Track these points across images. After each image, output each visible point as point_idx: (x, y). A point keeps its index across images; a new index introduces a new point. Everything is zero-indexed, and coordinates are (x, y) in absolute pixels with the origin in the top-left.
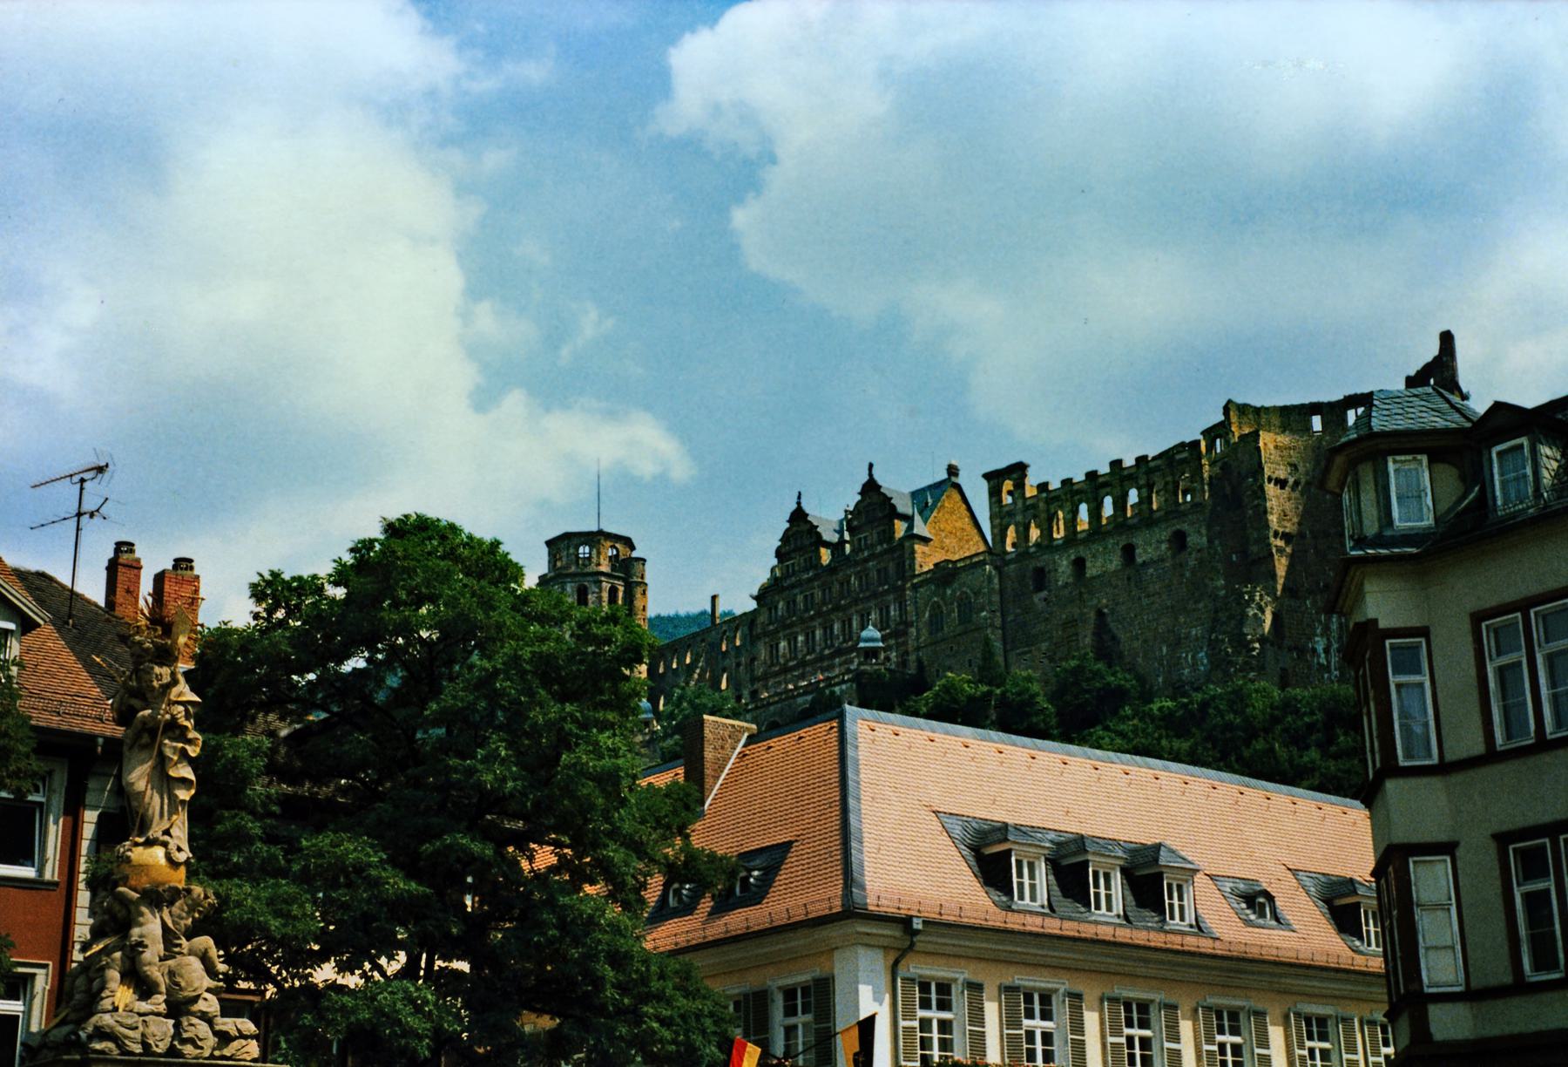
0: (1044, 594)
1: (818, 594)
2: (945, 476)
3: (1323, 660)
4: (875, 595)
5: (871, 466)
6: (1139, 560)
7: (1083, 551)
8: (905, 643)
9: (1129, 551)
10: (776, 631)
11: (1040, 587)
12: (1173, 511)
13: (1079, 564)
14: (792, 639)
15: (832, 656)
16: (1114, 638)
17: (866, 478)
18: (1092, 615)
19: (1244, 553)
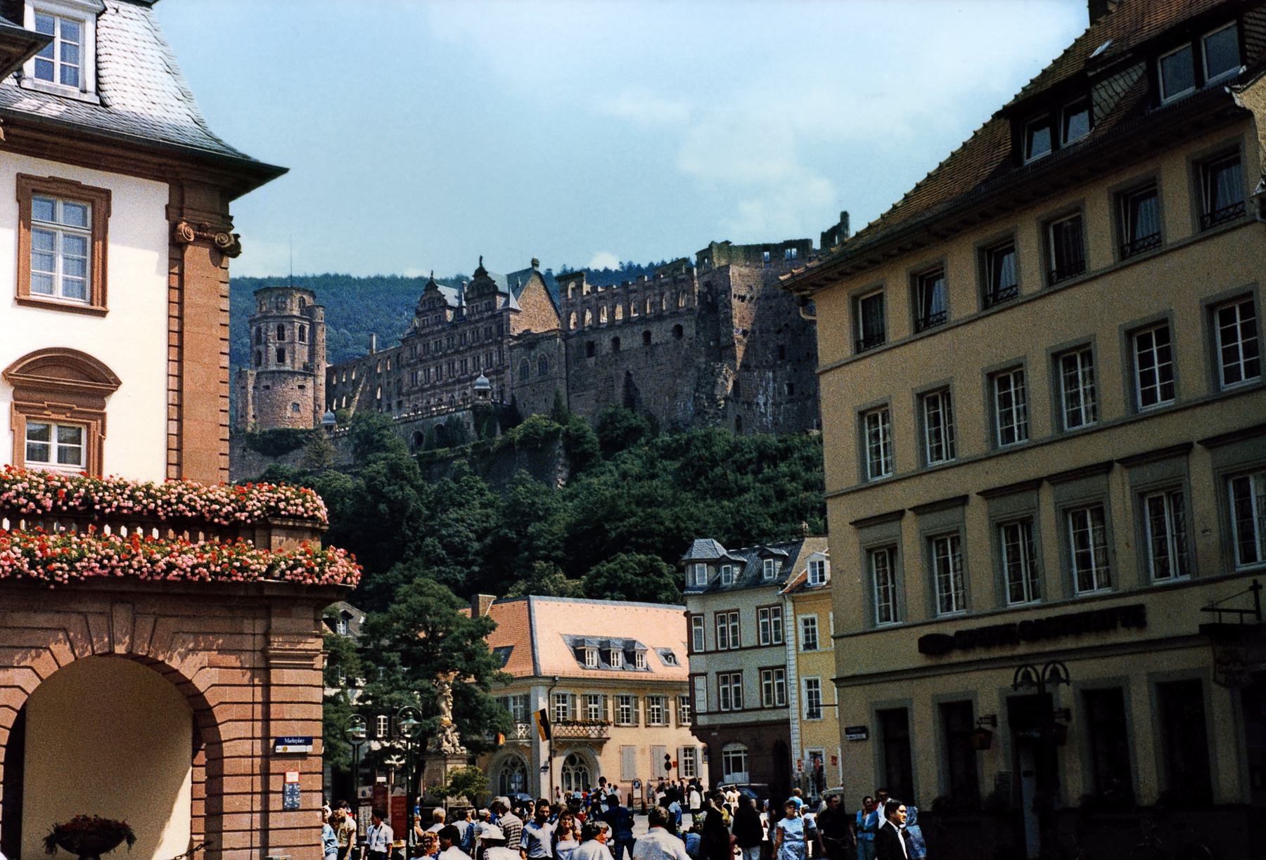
0: (592, 360)
1: (445, 342)
2: (530, 266)
3: (763, 410)
4: (482, 346)
5: (481, 258)
6: (653, 341)
7: (618, 333)
8: (502, 379)
9: (647, 335)
10: (416, 364)
11: (591, 354)
12: (675, 313)
13: (616, 341)
14: (427, 371)
15: (454, 383)
16: (636, 390)
17: (477, 266)
18: (624, 375)
19: (718, 340)
